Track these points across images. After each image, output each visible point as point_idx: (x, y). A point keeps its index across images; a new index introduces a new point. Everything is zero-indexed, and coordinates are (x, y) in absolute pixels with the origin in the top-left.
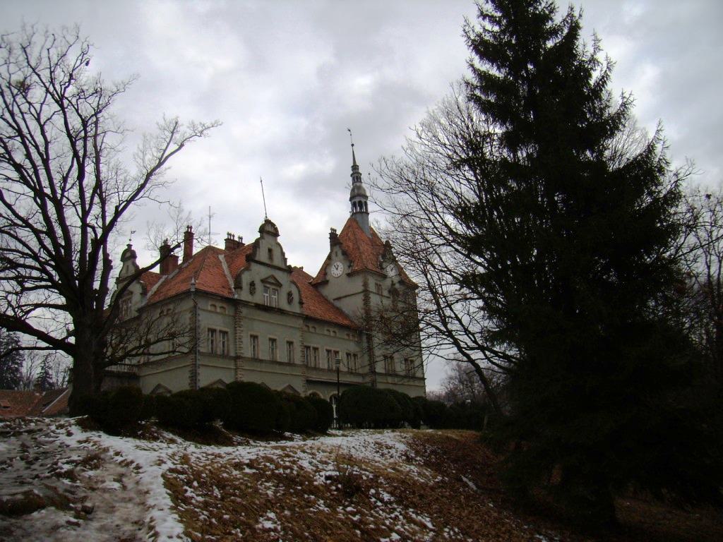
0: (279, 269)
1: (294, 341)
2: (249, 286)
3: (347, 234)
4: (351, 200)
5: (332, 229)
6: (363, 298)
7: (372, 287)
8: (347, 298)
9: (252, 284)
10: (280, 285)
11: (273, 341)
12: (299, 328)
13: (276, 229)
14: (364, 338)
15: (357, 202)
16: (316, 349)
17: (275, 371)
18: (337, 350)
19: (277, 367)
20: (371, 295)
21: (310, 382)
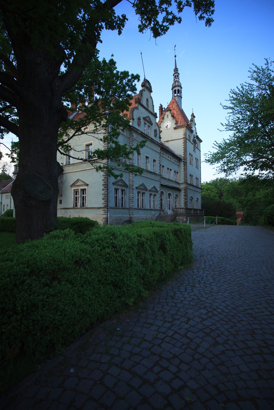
0: (152, 113)
1: (156, 159)
2: (137, 119)
3: (172, 107)
4: (172, 89)
5: (161, 104)
6: (183, 142)
7: (188, 138)
8: (173, 141)
9: (139, 119)
10: (152, 124)
11: (147, 158)
12: (158, 153)
13: (151, 87)
14: (182, 163)
15: (177, 90)
16: (163, 166)
17: (149, 177)
18: (171, 168)
19: (149, 174)
20: (187, 141)
21: (162, 185)
